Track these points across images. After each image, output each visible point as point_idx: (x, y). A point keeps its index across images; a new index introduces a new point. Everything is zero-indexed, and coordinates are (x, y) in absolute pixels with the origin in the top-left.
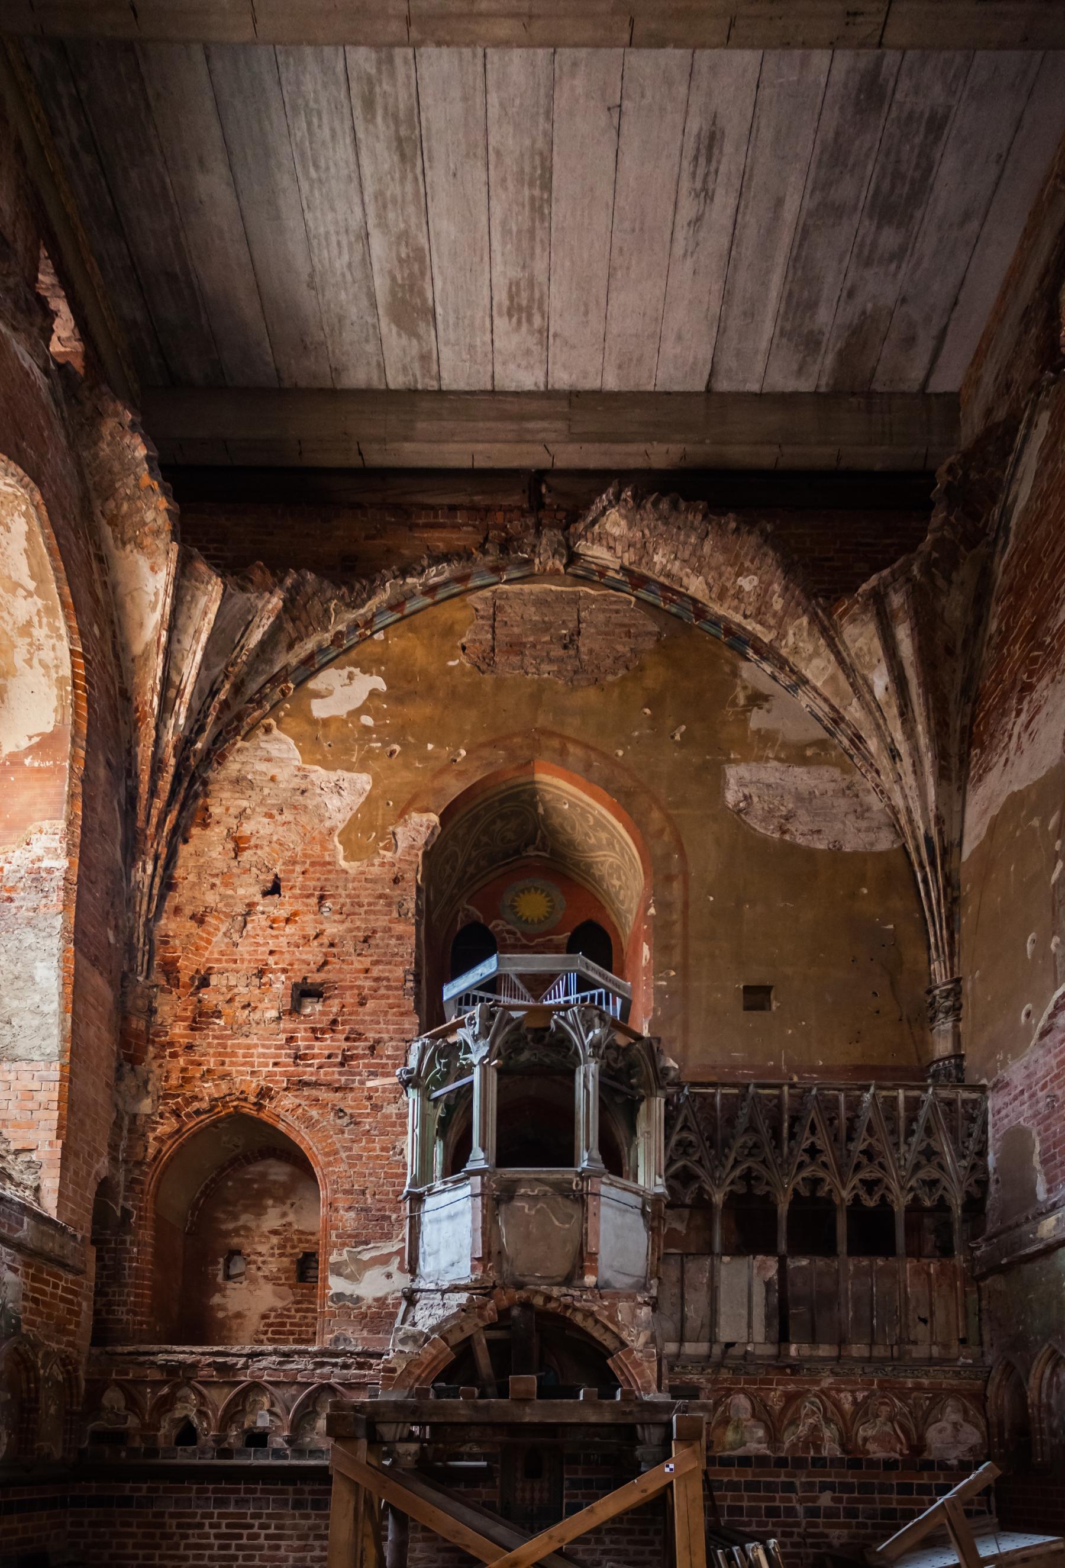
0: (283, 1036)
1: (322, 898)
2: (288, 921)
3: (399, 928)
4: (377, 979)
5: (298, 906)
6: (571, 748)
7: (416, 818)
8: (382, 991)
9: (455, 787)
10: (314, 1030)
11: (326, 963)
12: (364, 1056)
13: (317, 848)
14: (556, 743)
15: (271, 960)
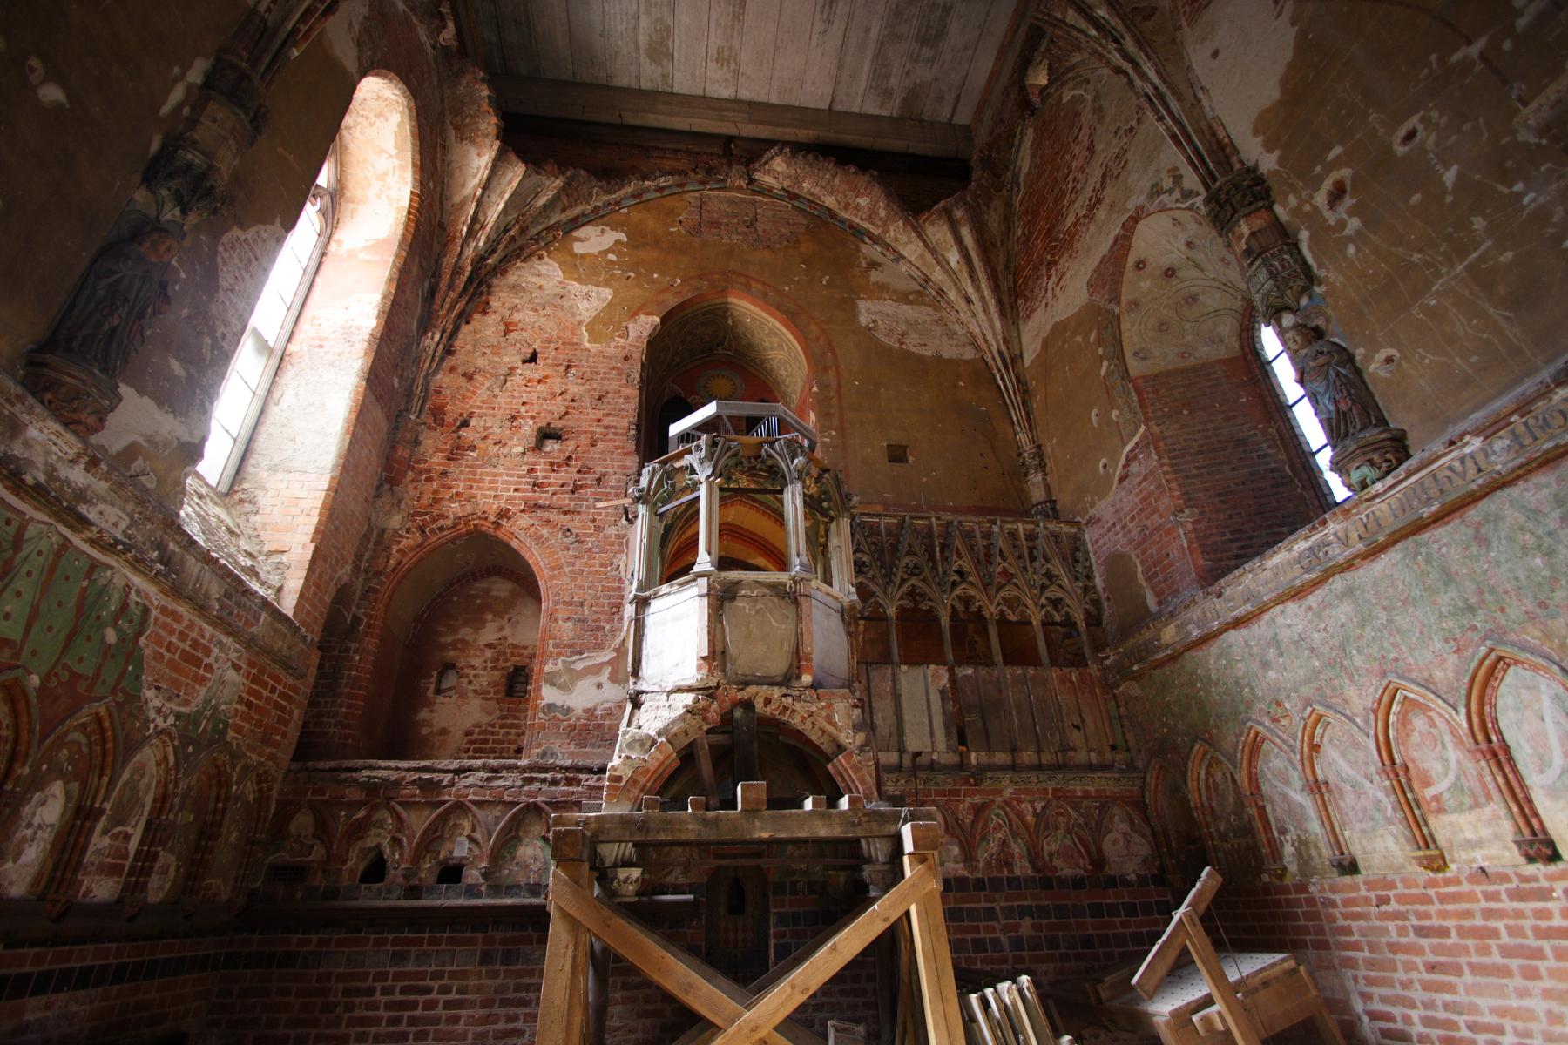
0: (526, 468)
1: (568, 367)
2: (540, 381)
3: (627, 391)
4: (606, 427)
5: (550, 371)
6: (754, 284)
7: (643, 318)
8: (610, 436)
9: (672, 301)
10: (552, 464)
11: (566, 413)
12: (591, 486)
13: (568, 334)
14: (742, 280)
15: (523, 409)
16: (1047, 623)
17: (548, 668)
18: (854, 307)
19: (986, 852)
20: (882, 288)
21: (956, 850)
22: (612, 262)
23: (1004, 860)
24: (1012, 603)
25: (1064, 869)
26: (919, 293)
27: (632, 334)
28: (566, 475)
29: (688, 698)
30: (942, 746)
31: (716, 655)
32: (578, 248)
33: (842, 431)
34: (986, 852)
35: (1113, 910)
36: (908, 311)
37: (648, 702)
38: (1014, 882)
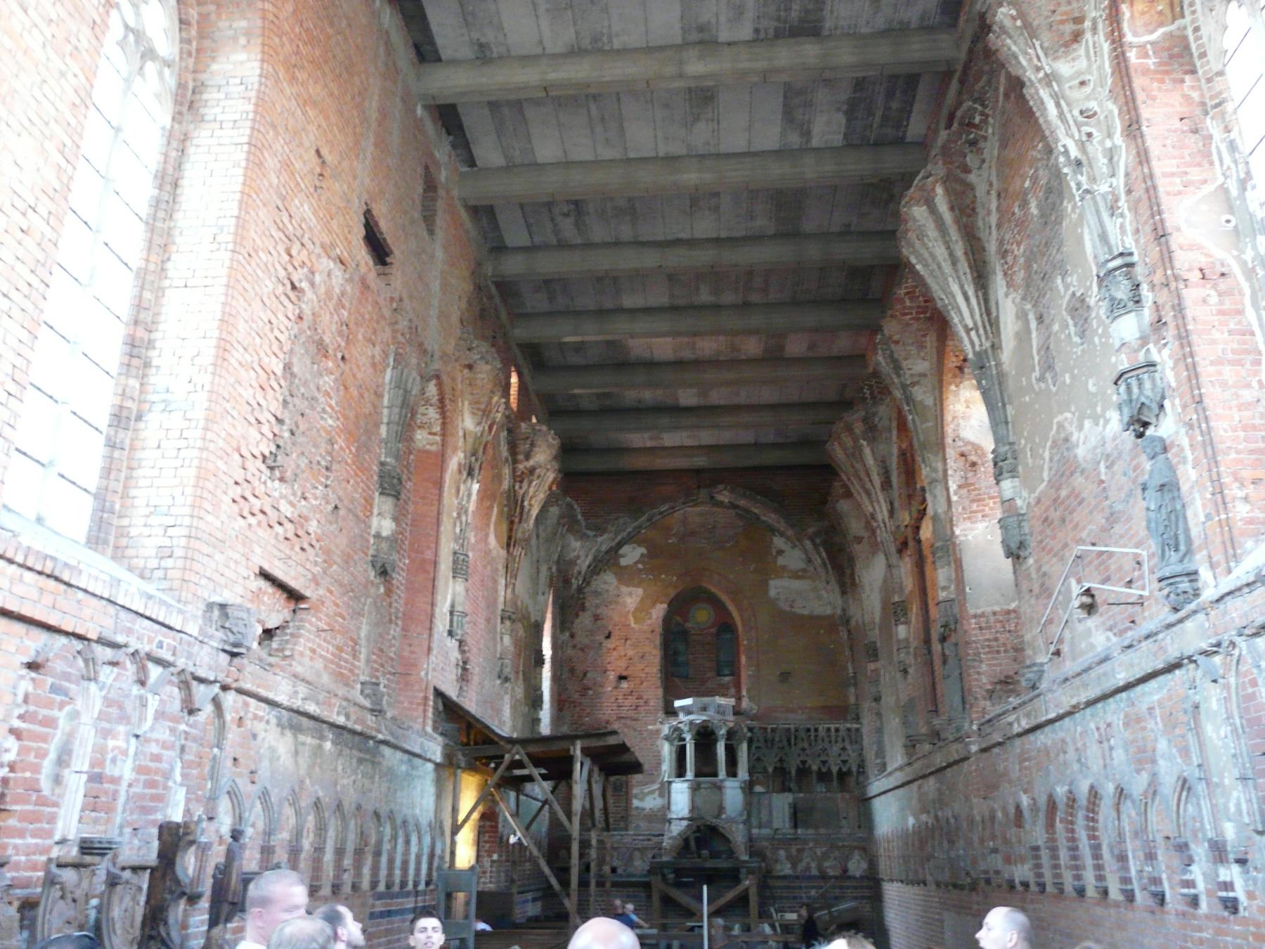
9: (672, 593)
16: (840, 772)
17: (635, 791)
18: (767, 585)
19: (800, 867)
20: (784, 568)
21: (789, 866)
22: (640, 570)
23: (808, 868)
24: (824, 762)
25: (831, 873)
26: (804, 570)
27: (654, 616)
28: (631, 701)
29: (685, 823)
30: (787, 825)
31: (693, 808)
32: (623, 562)
33: (758, 666)
34: (800, 867)
35: (848, 888)
36: (797, 584)
37: (674, 823)
38: (811, 878)
